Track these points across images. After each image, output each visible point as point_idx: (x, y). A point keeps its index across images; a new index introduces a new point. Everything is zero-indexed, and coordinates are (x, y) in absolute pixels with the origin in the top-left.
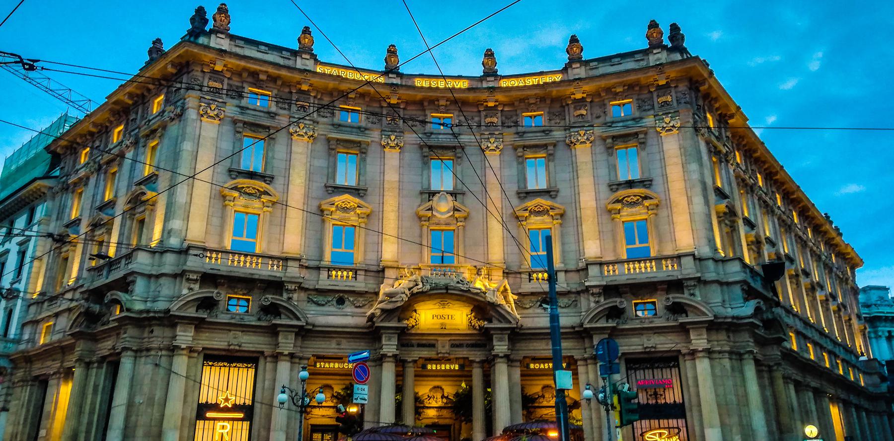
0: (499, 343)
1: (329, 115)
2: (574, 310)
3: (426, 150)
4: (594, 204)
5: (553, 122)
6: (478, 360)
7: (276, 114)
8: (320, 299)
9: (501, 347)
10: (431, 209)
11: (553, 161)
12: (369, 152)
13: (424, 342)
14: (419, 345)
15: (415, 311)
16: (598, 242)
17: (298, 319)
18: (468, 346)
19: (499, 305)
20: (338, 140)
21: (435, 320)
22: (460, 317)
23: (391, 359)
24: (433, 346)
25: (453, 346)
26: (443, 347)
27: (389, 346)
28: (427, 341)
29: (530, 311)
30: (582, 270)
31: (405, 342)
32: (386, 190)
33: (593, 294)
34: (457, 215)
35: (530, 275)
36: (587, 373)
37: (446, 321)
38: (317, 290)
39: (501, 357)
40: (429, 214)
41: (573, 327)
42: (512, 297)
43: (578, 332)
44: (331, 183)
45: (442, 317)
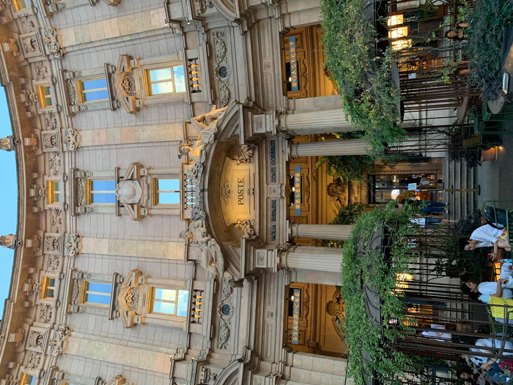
0: (264, 125)
1: (49, 311)
2: (228, 35)
3: (79, 210)
4: (114, 21)
5: (45, 75)
6: (288, 151)
7: (42, 370)
8: (223, 333)
9: (266, 124)
10: (132, 205)
11: (80, 72)
12: (84, 270)
13: (270, 213)
14: (274, 220)
15: (234, 224)
16: (152, 12)
17: (237, 371)
18: (273, 163)
19: (218, 128)
20: (70, 303)
21: (245, 201)
22: (240, 172)
23: (284, 258)
24: (274, 202)
25: (274, 180)
26: (275, 191)
27: (267, 259)
28: (266, 210)
29: (232, 89)
30: (182, 28)
31: (270, 236)
32: (116, 253)
33: (203, 10)
34: (135, 177)
35: (194, 92)
36: (298, 12)
37: (246, 188)
38: (212, 339)
39: (279, 122)
40: (135, 207)
41: (244, 33)
42: (214, 111)
43: (250, 28)
44: (108, 313)
45: (241, 193)
